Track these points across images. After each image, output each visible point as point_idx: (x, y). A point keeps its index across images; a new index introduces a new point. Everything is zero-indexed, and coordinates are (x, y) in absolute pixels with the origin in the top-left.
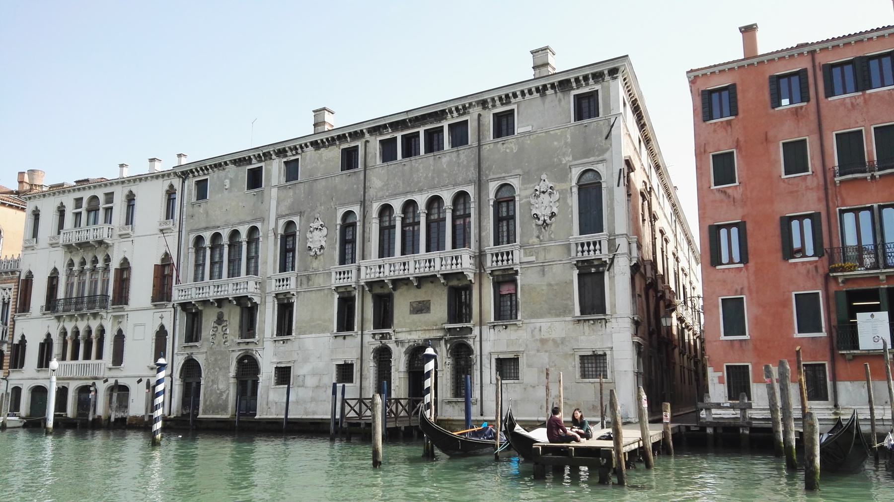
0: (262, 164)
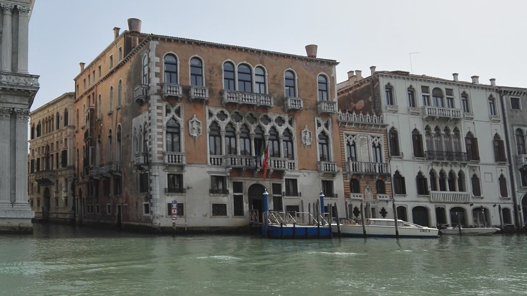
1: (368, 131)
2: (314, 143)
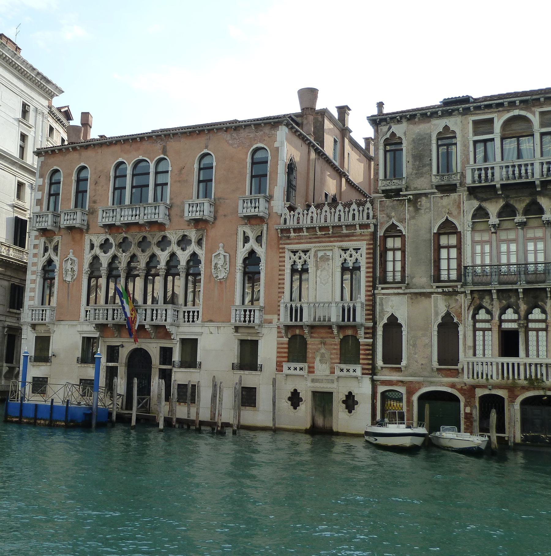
1: (336, 239)
2: (231, 273)
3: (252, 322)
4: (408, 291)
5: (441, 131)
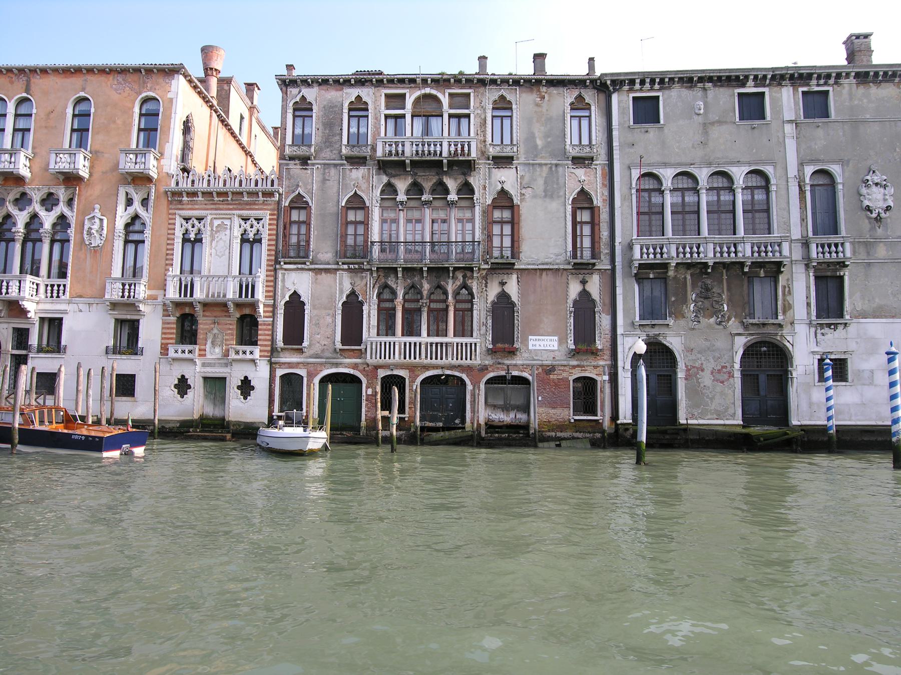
0: (766, 90)
1: (235, 206)
3: (132, 298)
4: (313, 266)
5: (354, 100)
